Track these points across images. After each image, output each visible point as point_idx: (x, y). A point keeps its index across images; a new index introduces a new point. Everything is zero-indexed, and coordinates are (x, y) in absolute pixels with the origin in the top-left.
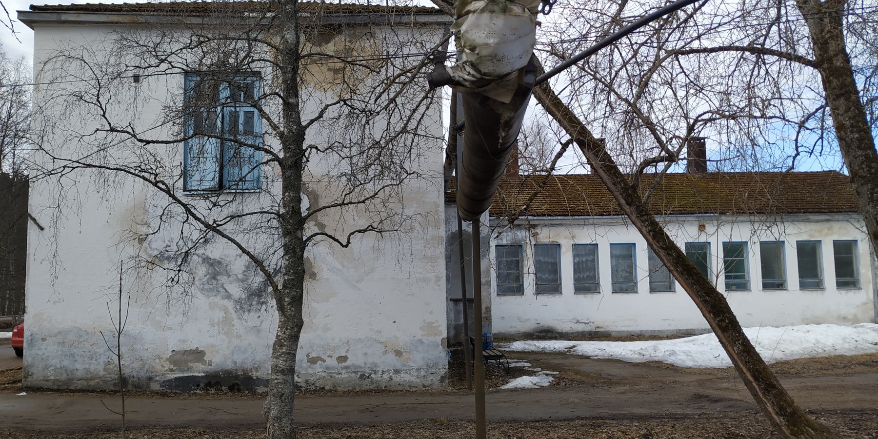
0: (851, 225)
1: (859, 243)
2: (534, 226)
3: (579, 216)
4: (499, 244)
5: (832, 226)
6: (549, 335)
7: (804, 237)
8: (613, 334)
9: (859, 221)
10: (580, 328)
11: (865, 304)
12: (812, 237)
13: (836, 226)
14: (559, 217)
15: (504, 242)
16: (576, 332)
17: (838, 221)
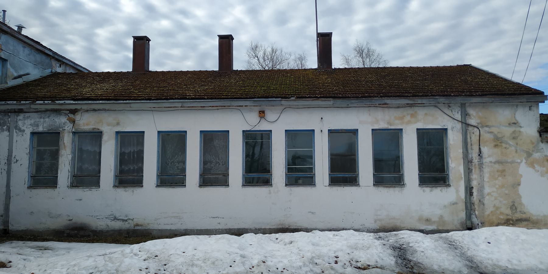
0: (440, 112)
1: (450, 132)
2: (74, 112)
3: (123, 100)
4: (34, 131)
5: (416, 112)
6: (82, 233)
7: (382, 125)
8: (154, 233)
9: (449, 106)
10: (117, 225)
11: (454, 204)
12: (391, 125)
13: (421, 112)
14: (101, 102)
15: (41, 129)
16: (112, 230)
17: (423, 105)
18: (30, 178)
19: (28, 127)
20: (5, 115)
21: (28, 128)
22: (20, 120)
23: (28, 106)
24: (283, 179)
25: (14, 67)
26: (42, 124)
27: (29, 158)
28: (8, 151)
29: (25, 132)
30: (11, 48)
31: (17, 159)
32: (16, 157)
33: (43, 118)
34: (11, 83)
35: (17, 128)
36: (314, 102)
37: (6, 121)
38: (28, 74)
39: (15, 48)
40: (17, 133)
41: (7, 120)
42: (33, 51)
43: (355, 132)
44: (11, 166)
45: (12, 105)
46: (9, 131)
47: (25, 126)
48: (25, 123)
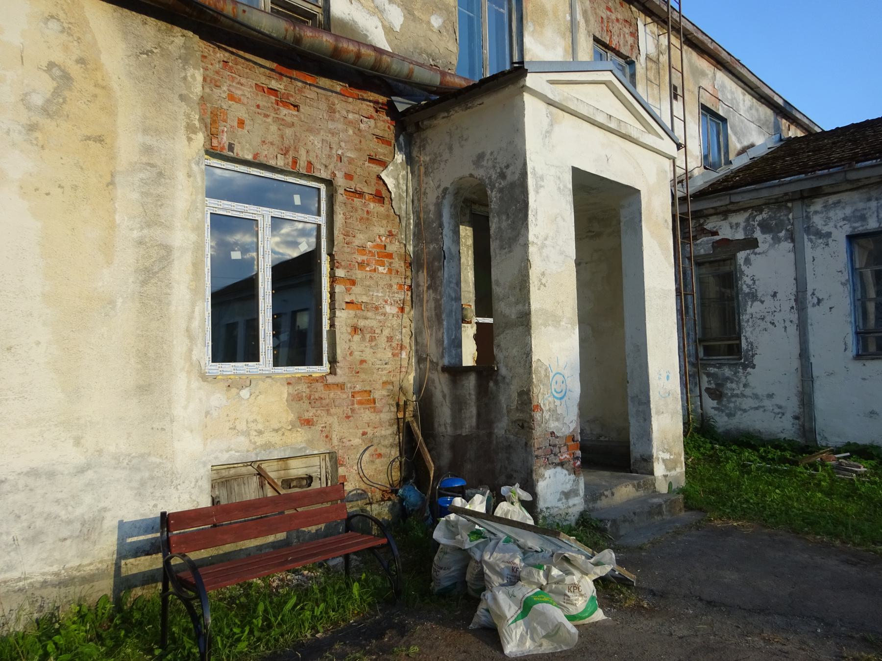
4: (856, 231)
21: (838, 227)
22: (816, 212)
23: (839, 178)
26: (876, 213)
28: (795, 282)
29: (833, 237)
31: (820, 298)
32: (815, 292)
33: (877, 199)
34: (738, 162)
38: (752, 146)
41: (785, 218)
44: (806, 314)
46: (793, 240)
47: (831, 224)
48: (829, 218)
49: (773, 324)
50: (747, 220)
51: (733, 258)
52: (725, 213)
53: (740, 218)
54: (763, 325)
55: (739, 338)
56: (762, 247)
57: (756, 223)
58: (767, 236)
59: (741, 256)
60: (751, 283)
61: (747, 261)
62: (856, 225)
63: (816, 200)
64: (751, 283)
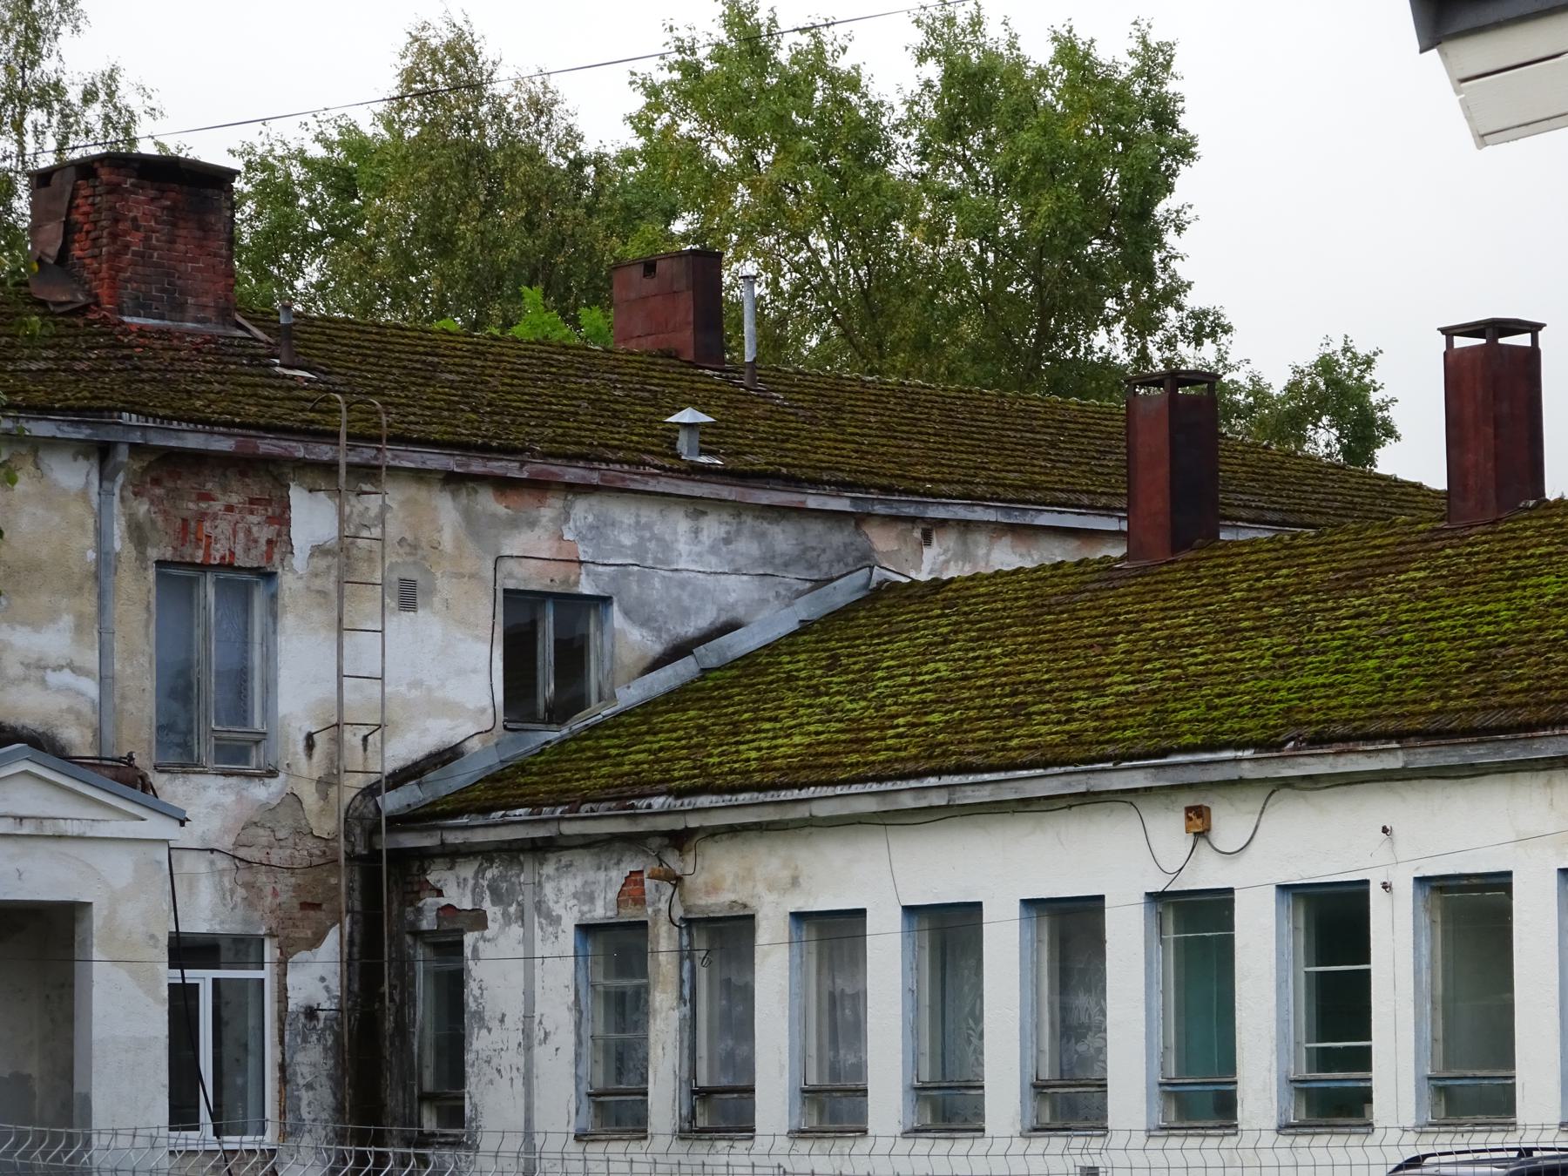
2: (680, 840)
14: (743, 798)
15: (600, 912)
18: (585, 1099)
19: (570, 904)
20: (511, 861)
22: (548, 877)
24: (1271, 1099)
25: (645, 621)
27: (578, 1025)
30: (627, 540)
33: (606, 869)
34: (630, 695)
35: (539, 906)
36: (1342, 759)
37: (513, 884)
38: (730, 627)
39: (648, 535)
40: (542, 929)
42: (749, 520)
43: (1501, 882)
45: (515, 825)
46: (523, 925)
47: (562, 902)
48: (560, 890)
49: (499, 1071)
50: (477, 873)
51: (461, 943)
52: (453, 855)
53: (467, 870)
54: (490, 1073)
55: (463, 1098)
56: (493, 928)
57: (485, 883)
58: (496, 909)
59: (469, 938)
60: (477, 992)
61: (475, 949)
62: (585, 908)
63: (549, 855)
64: (477, 992)
